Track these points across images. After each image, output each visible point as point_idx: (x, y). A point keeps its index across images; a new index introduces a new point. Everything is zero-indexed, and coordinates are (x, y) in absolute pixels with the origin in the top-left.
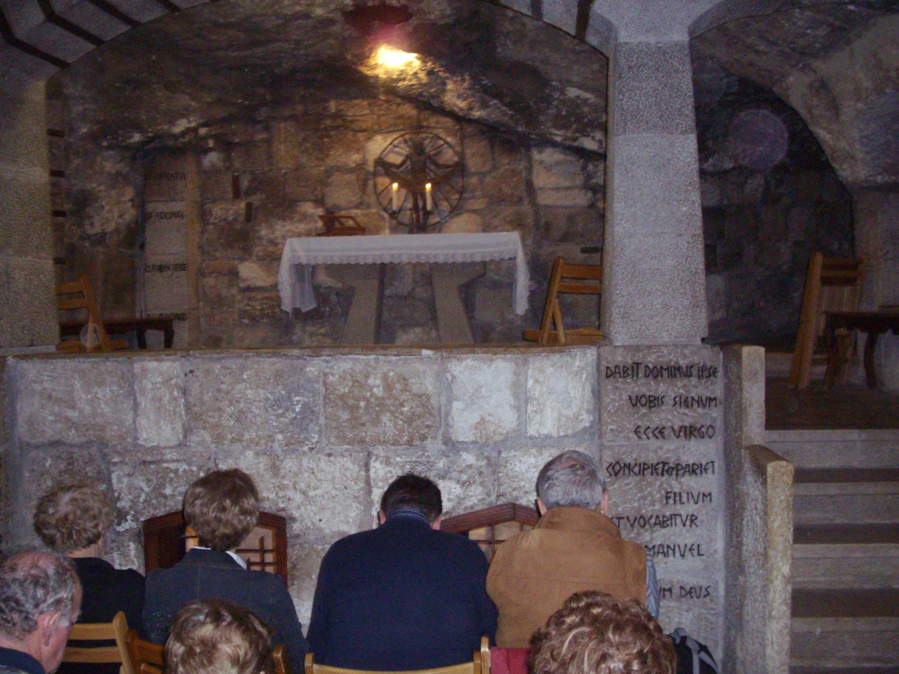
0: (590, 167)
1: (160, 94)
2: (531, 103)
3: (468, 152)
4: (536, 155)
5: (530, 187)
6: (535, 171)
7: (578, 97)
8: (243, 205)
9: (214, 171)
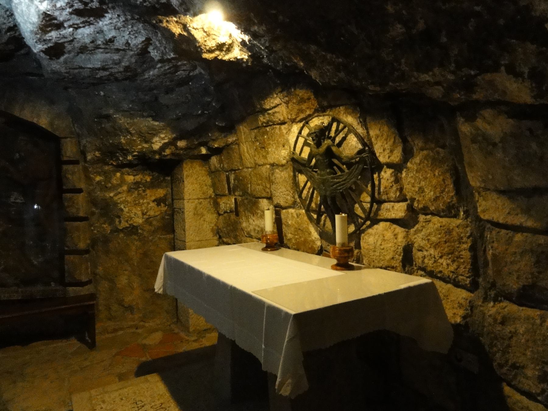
3: (373, 133)
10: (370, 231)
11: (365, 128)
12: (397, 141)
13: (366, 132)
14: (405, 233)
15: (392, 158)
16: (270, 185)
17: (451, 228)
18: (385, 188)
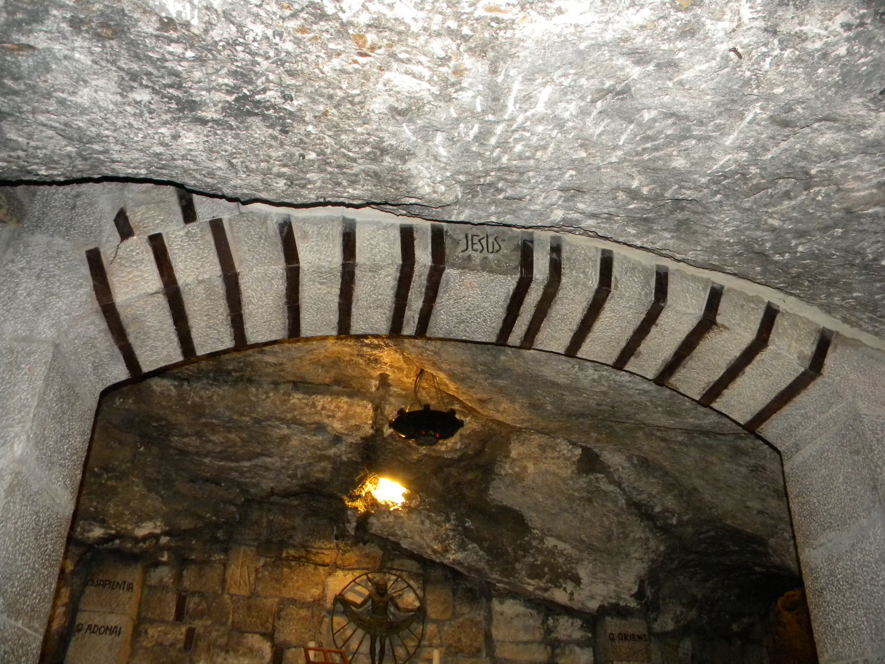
0: (550, 621)
1: (137, 489)
2: (510, 550)
3: (430, 598)
4: (496, 605)
5: (488, 637)
6: (495, 623)
7: (556, 547)
8: (184, 629)
9: (162, 587)
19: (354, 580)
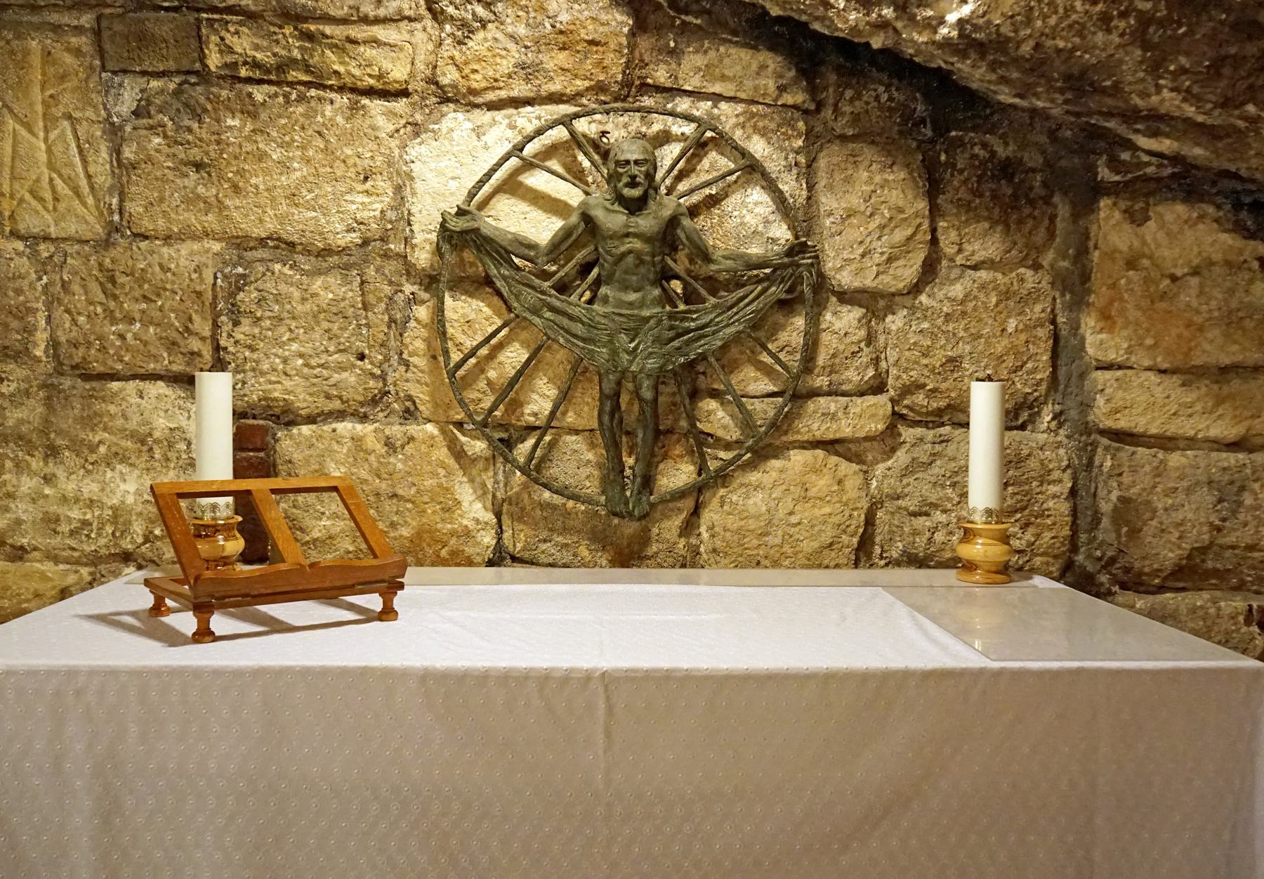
3: (827, 201)
10: (754, 477)
11: (804, 186)
12: (919, 237)
13: (805, 197)
14: (861, 475)
15: (885, 279)
16: (216, 326)
17: (1025, 452)
18: (834, 356)
19: (519, 148)
